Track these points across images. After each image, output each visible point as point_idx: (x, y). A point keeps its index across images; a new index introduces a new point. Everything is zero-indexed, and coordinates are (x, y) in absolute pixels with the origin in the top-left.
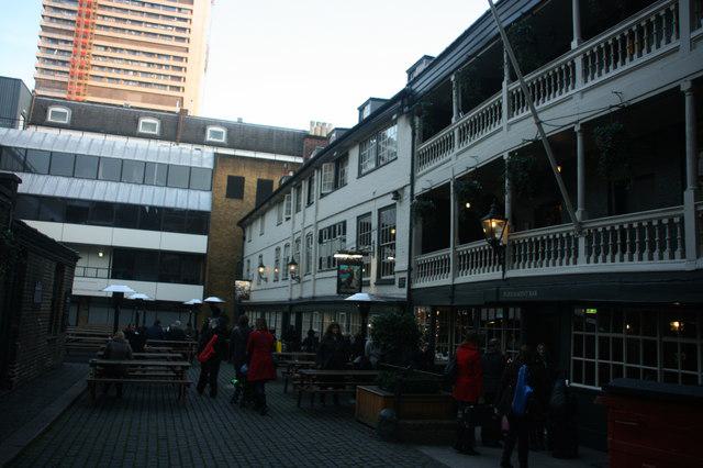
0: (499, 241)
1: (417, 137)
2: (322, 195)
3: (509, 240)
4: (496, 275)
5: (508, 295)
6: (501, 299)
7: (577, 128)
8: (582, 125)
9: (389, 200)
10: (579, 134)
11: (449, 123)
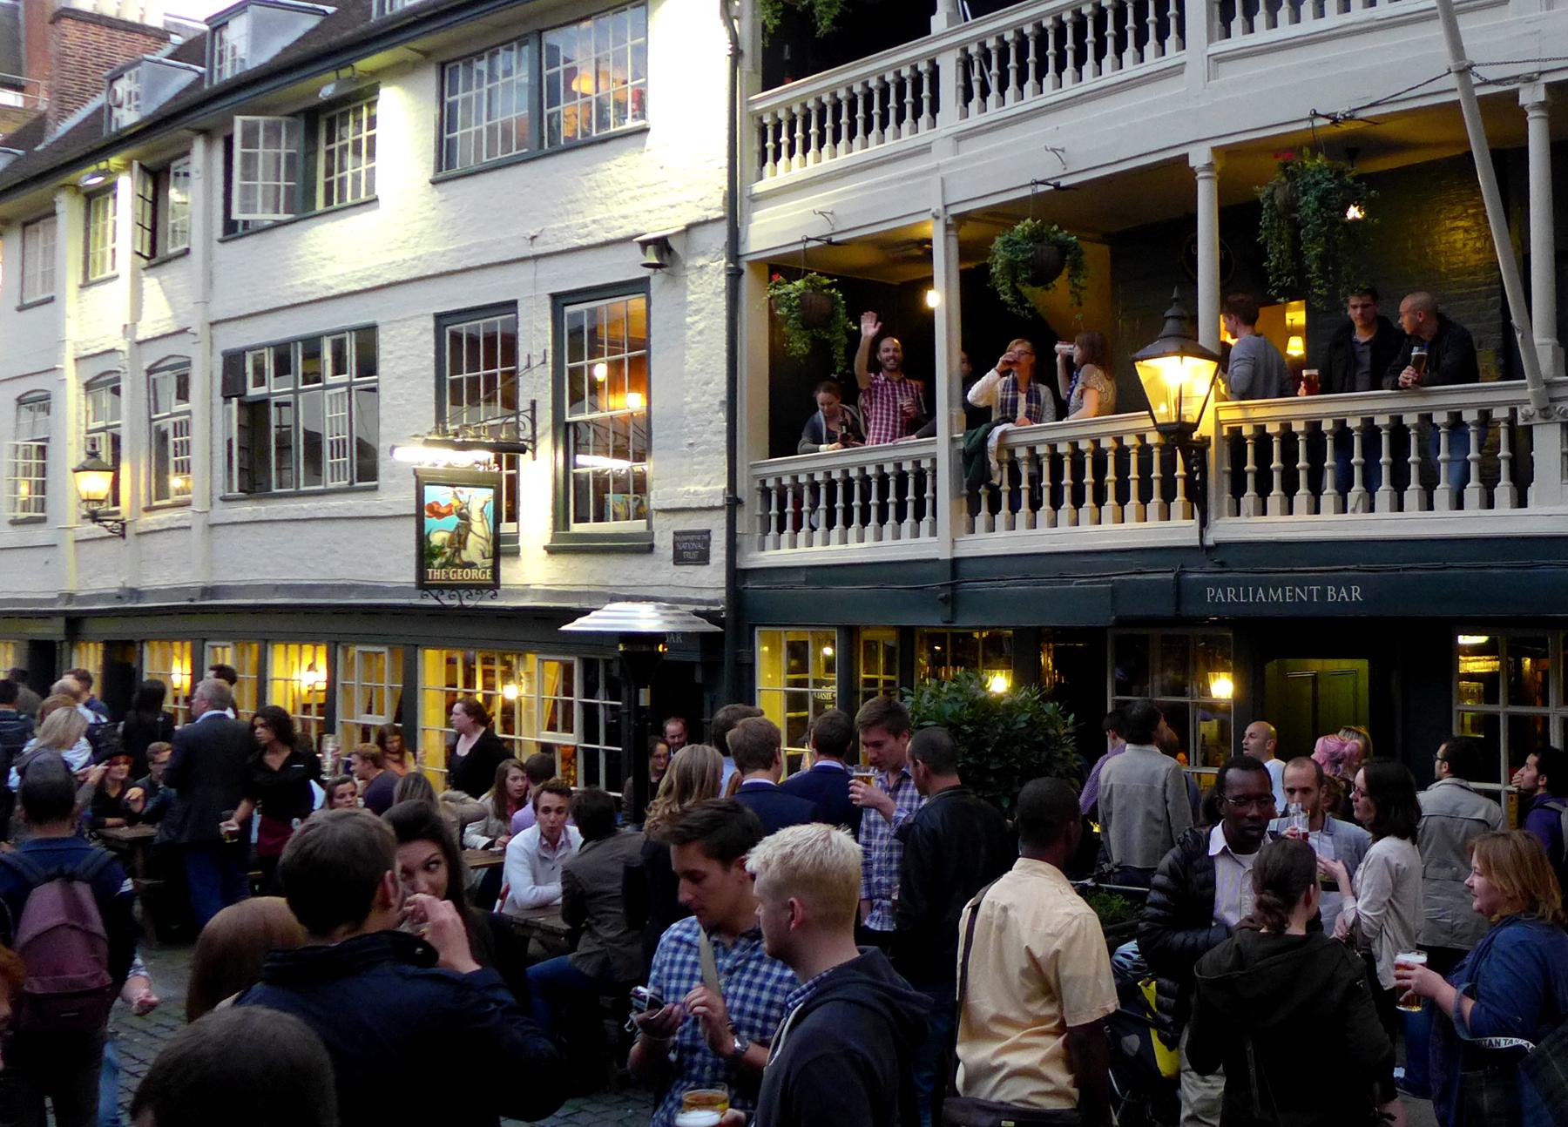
0: (1195, 426)
2: (232, 229)
3: (1219, 424)
4: (1179, 529)
5: (1222, 596)
6: (1190, 610)
7: (1531, 96)
8: (1550, 87)
9: (629, 265)
11: (925, 30)
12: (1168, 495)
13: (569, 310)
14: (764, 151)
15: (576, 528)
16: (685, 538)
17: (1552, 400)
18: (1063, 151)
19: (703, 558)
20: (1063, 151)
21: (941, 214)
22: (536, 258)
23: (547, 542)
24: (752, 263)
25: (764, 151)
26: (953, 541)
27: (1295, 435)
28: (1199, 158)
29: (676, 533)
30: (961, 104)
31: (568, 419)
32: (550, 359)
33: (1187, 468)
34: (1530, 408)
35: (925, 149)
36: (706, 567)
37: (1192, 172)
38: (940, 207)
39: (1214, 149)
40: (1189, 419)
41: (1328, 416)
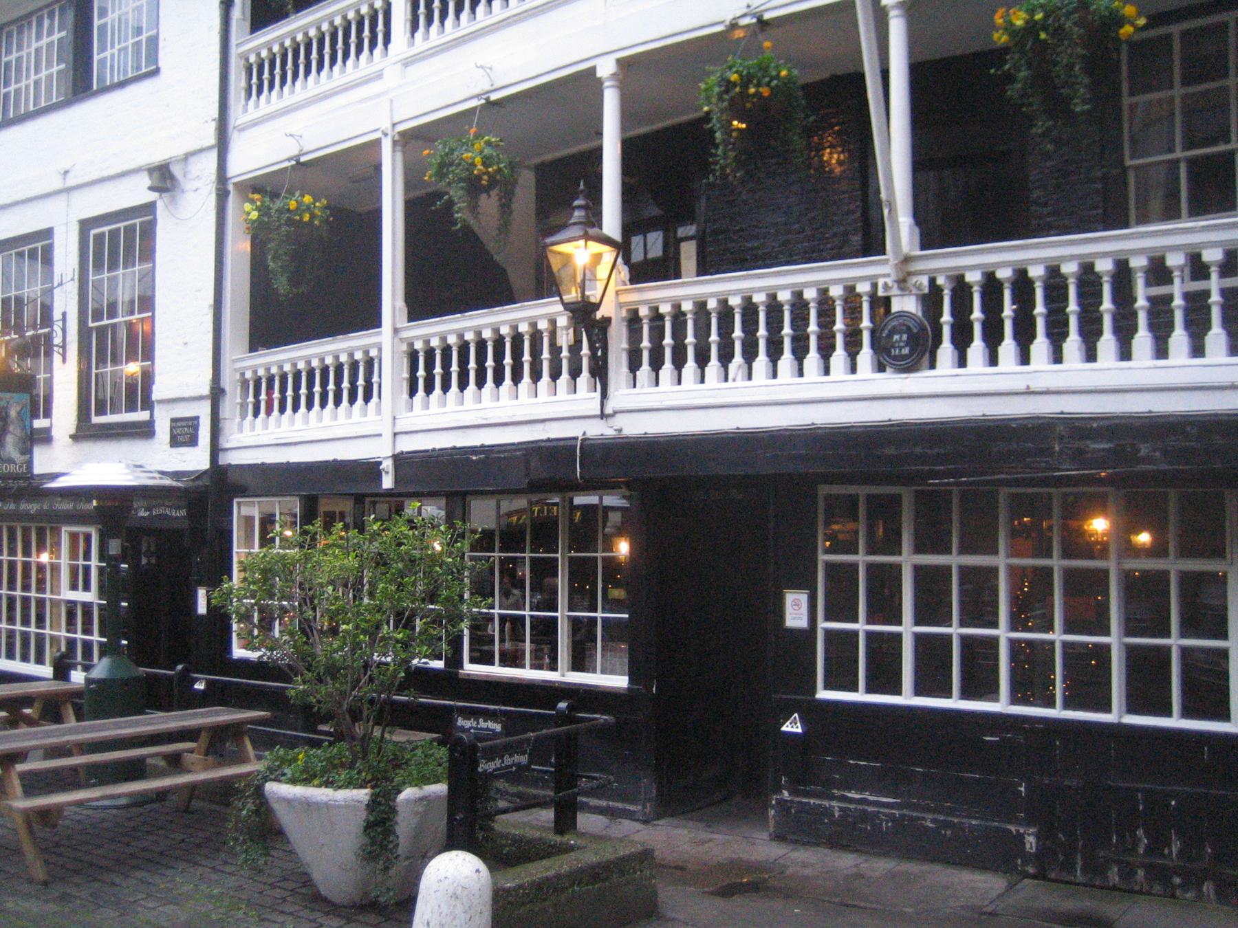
0: (597, 306)
1: (236, 13)
3: (620, 305)
10: (893, 13)
12: (575, 373)
13: (93, 232)
14: (250, 87)
15: (96, 420)
16: (179, 424)
17: (910, 274)
18: (491, 69)
19: (193, 441)
20: (491, 69)
21: (389, 131)
22: (68, 190)
23: (72, 431)
24: (236, 185)
25: (250, 87)
26: (394, 418)
27: (684, 314)
28: (606, 69)
29: (173, 420)
30: (408, 34)
31: (91, 324)
32: (76, 277)
33: (592, 348)
34: (889, 281)
35: (379, 76)
36: (196, 448)
37: (600, 82)
38: (386, 125)
39: (619, 61)
40: (593, 300)
41: (712, 295)
